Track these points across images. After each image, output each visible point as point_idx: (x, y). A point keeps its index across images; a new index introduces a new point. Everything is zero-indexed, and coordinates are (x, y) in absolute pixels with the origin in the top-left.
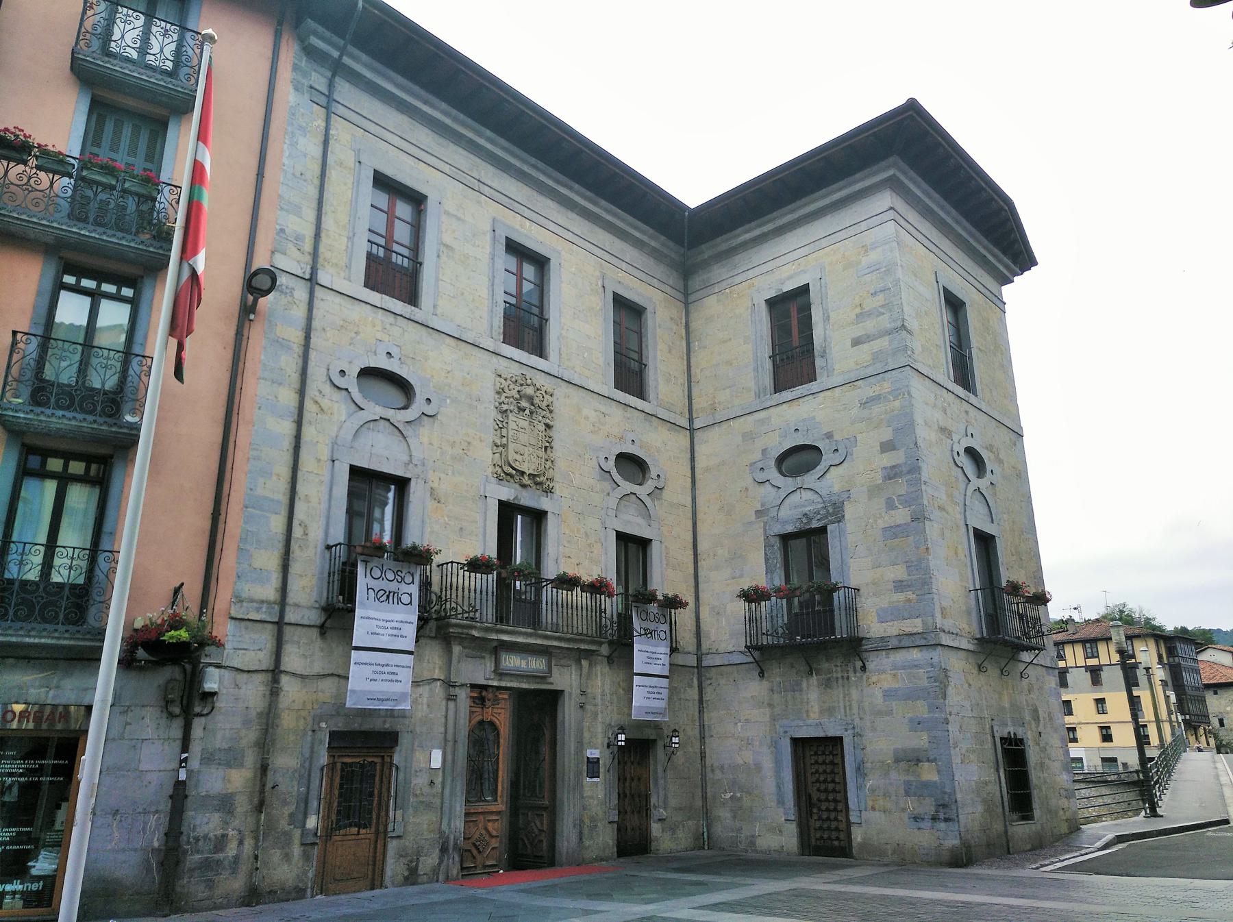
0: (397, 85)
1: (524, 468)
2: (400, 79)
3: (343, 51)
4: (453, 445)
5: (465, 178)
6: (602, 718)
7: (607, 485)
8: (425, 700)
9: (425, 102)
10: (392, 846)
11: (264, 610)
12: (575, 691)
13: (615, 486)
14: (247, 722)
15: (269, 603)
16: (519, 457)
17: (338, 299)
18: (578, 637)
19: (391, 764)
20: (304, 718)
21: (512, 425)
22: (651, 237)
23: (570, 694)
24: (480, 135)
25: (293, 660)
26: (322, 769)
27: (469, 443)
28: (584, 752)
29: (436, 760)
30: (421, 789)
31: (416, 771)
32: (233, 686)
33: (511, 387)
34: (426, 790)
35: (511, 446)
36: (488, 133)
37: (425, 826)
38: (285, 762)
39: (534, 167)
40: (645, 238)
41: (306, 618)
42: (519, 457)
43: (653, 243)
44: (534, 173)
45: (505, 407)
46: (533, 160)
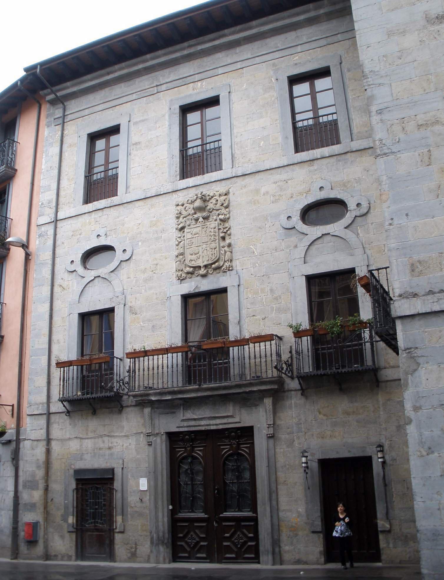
0: (91, 80)
1: (200, 263)
3: (53, 92)
4: (144, 271)
5: (147, 92)
7: (294, 239)
9: (108, 74)
13: (302, 236)
14: (38, 467)
15: (43, 404)
16: (194, 257)
17: (70, 221)
20: (64, 463)
22: (316, 9)
24: (147, 61)
25: (56, 433)
26: (73, 491)
27: (157, 265)
29: (143, 484)
31: (131, 492)
32: (31, 449)
34: (139, 504)
35: (188, 252)
36: (148, 56)
37: (140, 527)
38: (57, 487)
39: (190, 46)
40: (312, 14)
41: (60, 408)
43: (322, 11)
44: (192, 50)
46: (186, 44)
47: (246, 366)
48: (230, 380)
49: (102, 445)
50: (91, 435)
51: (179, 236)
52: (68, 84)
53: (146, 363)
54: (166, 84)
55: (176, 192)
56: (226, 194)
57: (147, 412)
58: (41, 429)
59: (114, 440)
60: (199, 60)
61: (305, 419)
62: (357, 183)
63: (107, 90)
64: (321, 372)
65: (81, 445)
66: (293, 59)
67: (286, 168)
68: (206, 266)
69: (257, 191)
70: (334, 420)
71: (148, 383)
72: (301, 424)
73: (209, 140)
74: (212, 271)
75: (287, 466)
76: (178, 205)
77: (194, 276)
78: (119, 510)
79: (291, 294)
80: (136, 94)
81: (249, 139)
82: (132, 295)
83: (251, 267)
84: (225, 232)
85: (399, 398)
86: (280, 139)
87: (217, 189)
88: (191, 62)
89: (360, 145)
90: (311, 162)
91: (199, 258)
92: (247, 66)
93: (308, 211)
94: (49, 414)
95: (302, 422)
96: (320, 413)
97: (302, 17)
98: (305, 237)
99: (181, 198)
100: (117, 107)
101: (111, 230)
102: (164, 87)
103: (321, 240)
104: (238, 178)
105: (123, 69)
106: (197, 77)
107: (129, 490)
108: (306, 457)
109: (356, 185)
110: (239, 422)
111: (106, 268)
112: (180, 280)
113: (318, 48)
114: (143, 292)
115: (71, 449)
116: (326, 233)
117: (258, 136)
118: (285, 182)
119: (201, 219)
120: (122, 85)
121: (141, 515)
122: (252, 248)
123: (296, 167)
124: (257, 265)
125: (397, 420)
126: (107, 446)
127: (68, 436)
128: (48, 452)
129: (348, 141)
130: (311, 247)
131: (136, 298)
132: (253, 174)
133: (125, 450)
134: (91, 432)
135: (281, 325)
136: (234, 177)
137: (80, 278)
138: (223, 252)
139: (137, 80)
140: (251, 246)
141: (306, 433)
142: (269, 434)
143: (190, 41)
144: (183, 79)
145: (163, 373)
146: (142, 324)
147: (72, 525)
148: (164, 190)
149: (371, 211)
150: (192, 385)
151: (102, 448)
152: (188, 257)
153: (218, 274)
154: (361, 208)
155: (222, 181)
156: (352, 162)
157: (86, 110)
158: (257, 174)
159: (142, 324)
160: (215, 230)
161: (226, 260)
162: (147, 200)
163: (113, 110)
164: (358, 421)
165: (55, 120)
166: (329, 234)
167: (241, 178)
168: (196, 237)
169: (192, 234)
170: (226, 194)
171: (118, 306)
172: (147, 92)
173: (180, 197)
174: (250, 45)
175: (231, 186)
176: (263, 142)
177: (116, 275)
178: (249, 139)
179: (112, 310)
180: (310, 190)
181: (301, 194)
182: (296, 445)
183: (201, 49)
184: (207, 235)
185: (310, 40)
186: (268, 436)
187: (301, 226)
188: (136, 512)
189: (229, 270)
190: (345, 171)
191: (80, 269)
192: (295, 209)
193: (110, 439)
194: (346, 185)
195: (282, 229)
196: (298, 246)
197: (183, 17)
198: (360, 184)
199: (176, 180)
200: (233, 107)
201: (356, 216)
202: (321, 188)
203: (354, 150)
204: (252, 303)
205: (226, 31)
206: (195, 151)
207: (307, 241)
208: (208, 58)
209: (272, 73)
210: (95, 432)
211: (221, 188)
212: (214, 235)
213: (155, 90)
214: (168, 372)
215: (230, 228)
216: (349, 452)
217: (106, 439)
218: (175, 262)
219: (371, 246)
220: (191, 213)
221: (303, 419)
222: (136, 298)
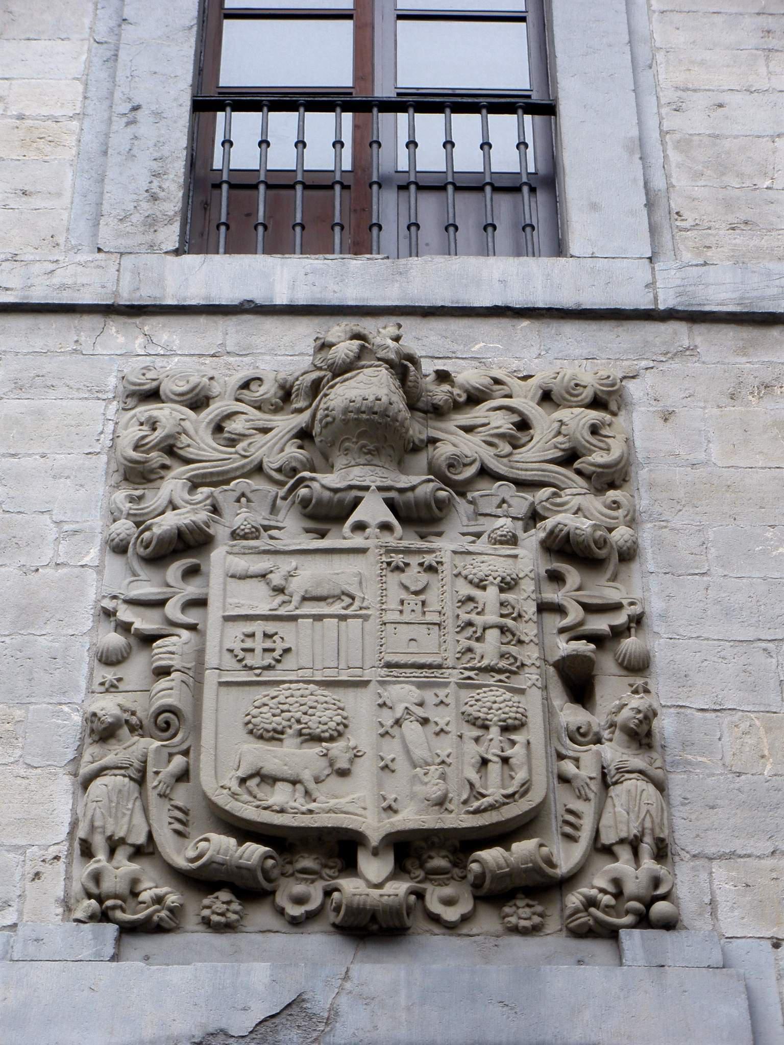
33: (236, 426)
74: (465, 906)
76: (153, 395)
77: (261, 916)
91: (343, 773)
112: (111, 930)
136: (670, 315)
153: (516, 939)
161: (608, 838)
168: (319, 618)
169: (280, 590)
170: (597, 403)
175: (644, 364)
189: (644, 921)
199: (152, 247)
212: (503, 630)
218: (65, 782)
220: (272, 462)
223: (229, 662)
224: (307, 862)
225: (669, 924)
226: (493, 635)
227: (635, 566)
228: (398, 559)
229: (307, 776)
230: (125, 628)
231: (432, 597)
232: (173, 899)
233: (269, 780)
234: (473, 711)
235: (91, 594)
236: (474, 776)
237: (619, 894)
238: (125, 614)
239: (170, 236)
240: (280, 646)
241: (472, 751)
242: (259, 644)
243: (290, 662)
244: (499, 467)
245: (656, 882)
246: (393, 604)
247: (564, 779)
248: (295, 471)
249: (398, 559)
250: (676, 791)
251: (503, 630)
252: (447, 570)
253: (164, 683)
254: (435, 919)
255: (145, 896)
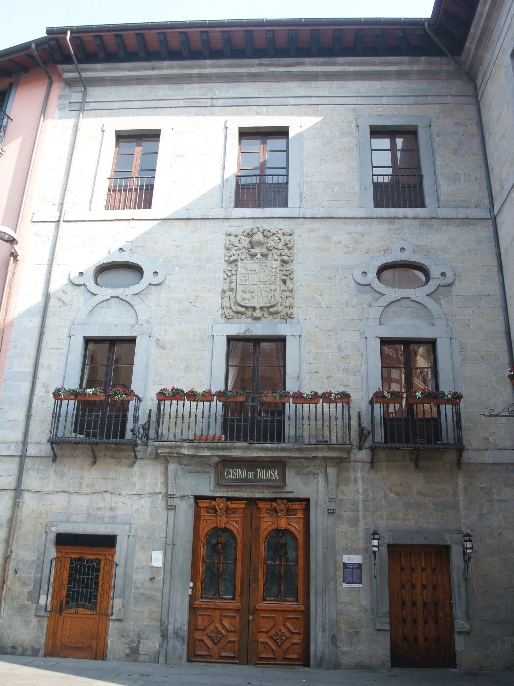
0: (129, 70)
1: (255, 303)
2: (127, 65)
3: (77, 70)
4: (180, 301)
5: (199, 102)
6: (366, 524)
7: (368, 297)
8: (147, 510)
9: (153, 69)
10: (112, 626)
11: (12, 448)
12: (322, 497)
13: (378, 296)
15: (17, 443)
16: (248, 296)
18: (310, 446)
19: (112, 561)
20: (41, 524)
21: (241, 270)
22: (409, 64)
23: (316, 501)
24: (205, 67)
26: (51, 561)
27: (197, 296)
28: (338, 557)
30: (143, 583)
31: (137, 568)
34: (148, 585)
35: (239, 289)
36: (208, 62)
37: (146, 615)
39: (261, 65)
40: (405, 68)
41: (43, 451)
42: (248, 296)
43: (415, 68)
44: (262, 70)
45: (232, 259)
46: (257, 61)
47: (304, 428)
48: (284, 441)
49: (101, 504)
50: (85, 489)
51: (230, 269)
52: (98, 66)
53: (180, 408)
54: (223, 99)
55: (228, 220)
56: (290, 234)
57: (173, 468)
58: (9, 476)
59: (121, 499)
60: (266, 83)
61: (374, 496)
62: (441, 251)
63: (146, 87)
64: (390, 445)
65: (69, 502)
66: (377, 109)
67: (363, 220)
68: (261, 308)
69: (328, 238)
70: (407, 500)
71: (175, 432)
72: (368, 501)
73: (268, 172)
75: (350, 550)
78: (118, 590)
79: (362, 354)
80: (185, 100)
81: (321, 181)
82: (161, 326)
83: (316, 319)
84: (287, 275)
85: (482, 484)
86: (357, 189)
87: (280, 227)
88: (256, 84)
89: (448, 213)
90: (392, 220)
92: (323, 104)
93: (383, 271)
94: (23, 457)
95: (370, 500)
96: (391, 491)
97: (393, 68)
98: (380, 297)
99: (234, 227)
100: (157, 109)
101: (139, 247)
102: (220, 102)
103: (398, 304)
104: (305, 220)
105: (172, 68)
106: (262, 101)
107: (135, 565)
108: (378, 539)
109: (440, 254)
110: (293, 492)
111: (128, 289)
113: (406, 104)
114: (176, 325)
115: (54, 506)
116: (406, 297)
117: (332, 181)
118: (361, 235)
119: (259, 256)
120: (167, 86)
121: (150, 598)
122: (318, 298)
123: (375, 222)
124: (323, 317)
125: (479, 507)
126: (108, 506)
127: (51, 488)
128: (16, 506)
129: (435, 207)
130: (387, 309)
131: (166, 331)
132: (324, 219)
133: (134, 513)
134: (88, 486)
135: (348, 387)
136: (302, 218)
137: (89, 295)
138: (284, 297)
139: (186, 86)
140: (317, 296)
141: (374, 512)
142: (331, 510)
143: (262, 59)
144: (245, 100)
145: (196, 422)
146: (171, 361)
147: (44, 608)
148: (213, 215)
149: (456, 282)
150: (242, 441)
151: (101, 508)
152: (240, 295)
154: (445, 278)
155: (285, 219)
156: (437, 228)
157: (116, 103)
158: (329, 220)
159: (171, 361)
160: (276, 270)
162: (189, 221)
163: (152, 112)
164: (434, 505)
165: (72, 104)
166: (409, 298)
167: (309, 220)
168: (251, 274)
170: (290, 234)
171: (141, 336)
172: (199, 102)
173: (233, 226)
174: (327, 82)
175: (297, 227)
176: (337, 188)
177: (141, 299)
178: (321, 181)
179: (132, 340)
180: (388, 249)
181: (378, 251)
182: (362, 525)
183: (273, 72)
184: (266, 274)
185: (397, 94)
186: (329, 511)
187: (376, 284)
188: (143, 595)
189: (290, 318)
190: (429, 236)
191: (92, 286)
192: (371, 265)
193: (114, 497)
194: (430, 251)
195: (354, 283)
196: (372, 305)
197: (266, 28)
198: (445, 253)
199: (230, 207)
200: (304, 144)
201: (439, 285)
202: (403, 249)
203: (440, 217)
204: (315, 359)
205: (307, 60)
206: (249, 182)
207: (383, 302)
208: (277, 84)
209: (351, 118)
210: (92, 486)
211: (285, 226)
212: (275, 276)
213: (209, 102)
214: (202, 423)
215: (292, 272)
216: (426, 538)
217: (107, 496)
219: (454, 318)
221: (371, 496)
222: (166, 331)
223: (240, 281)
224: (250, 310)
225: (292, 318)
226: (274, 277)
227: (293, 262)
228: (262, 264)
229: (249, 299)
230: (227, 274)
231: (266, 270)
232: (234, 315)
233: (245, 299)
234: (270, 289)
235: (223, 269)
236: (270, 299)
237: (287, 314)
238: (227, 272)
239: (233, 204)
240: (246, 278)
241: (270, 295)
242: (244, 278)
243: (248, 281)
244: (276, 247)
245: (291, 313)
246: (261, 272)
247: (281, 297)
248: (249, 248)
249: (262, 264)
250: (295, 298)
251: (275, 276)
252: (268, 266)
253: (232, 284)
254: (265, 317)
255: (230, 315)
